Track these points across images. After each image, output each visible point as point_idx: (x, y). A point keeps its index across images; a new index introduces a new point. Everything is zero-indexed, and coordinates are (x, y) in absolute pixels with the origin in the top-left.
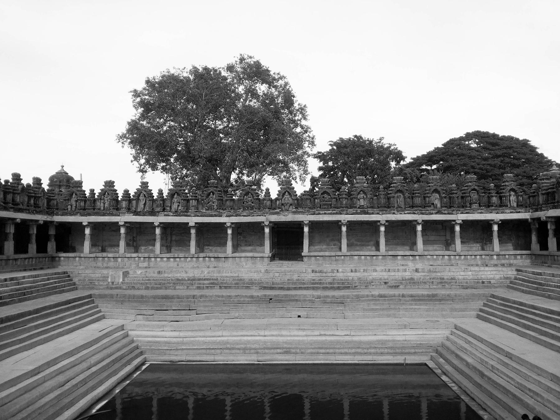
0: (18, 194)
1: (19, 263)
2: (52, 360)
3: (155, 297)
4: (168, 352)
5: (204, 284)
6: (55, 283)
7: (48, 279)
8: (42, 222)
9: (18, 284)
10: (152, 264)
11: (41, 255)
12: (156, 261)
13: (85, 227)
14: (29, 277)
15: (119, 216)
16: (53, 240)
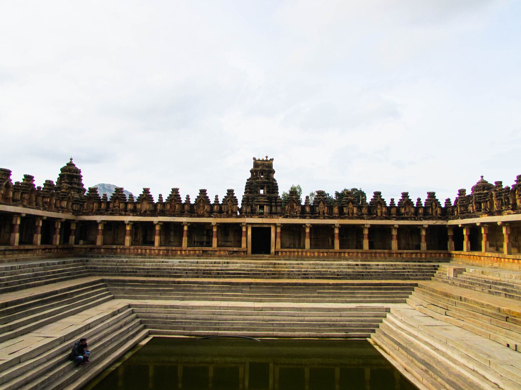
0: (402, 207)
1: (404, 256)
2: (275, 307)
3: (442, 293)
4: (383, 336)
5: (499, 289)
6: (409, 272)
7: (404, 269)
8: (426, 226)
9: (366, 268)
10: (501, 264)
11: (430, 251)
12: (505, 261)
13: (461, 229)
14: (383, 265)
15: (479, 217)
16: (450, 240)
